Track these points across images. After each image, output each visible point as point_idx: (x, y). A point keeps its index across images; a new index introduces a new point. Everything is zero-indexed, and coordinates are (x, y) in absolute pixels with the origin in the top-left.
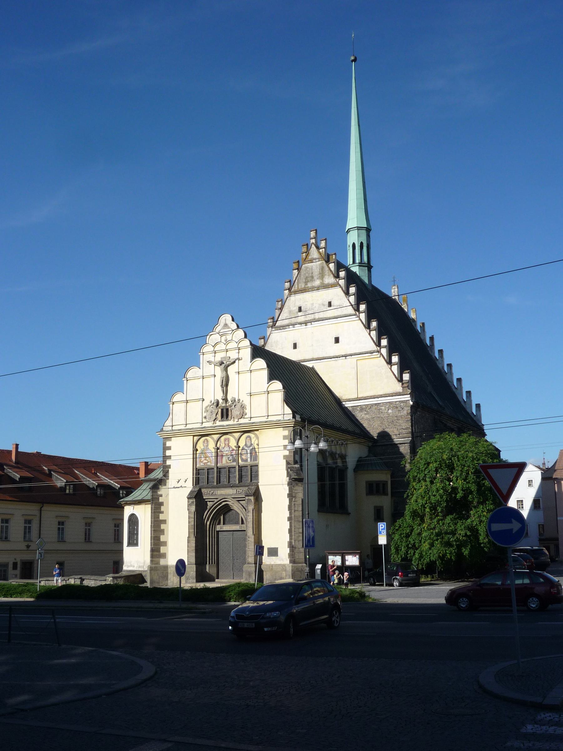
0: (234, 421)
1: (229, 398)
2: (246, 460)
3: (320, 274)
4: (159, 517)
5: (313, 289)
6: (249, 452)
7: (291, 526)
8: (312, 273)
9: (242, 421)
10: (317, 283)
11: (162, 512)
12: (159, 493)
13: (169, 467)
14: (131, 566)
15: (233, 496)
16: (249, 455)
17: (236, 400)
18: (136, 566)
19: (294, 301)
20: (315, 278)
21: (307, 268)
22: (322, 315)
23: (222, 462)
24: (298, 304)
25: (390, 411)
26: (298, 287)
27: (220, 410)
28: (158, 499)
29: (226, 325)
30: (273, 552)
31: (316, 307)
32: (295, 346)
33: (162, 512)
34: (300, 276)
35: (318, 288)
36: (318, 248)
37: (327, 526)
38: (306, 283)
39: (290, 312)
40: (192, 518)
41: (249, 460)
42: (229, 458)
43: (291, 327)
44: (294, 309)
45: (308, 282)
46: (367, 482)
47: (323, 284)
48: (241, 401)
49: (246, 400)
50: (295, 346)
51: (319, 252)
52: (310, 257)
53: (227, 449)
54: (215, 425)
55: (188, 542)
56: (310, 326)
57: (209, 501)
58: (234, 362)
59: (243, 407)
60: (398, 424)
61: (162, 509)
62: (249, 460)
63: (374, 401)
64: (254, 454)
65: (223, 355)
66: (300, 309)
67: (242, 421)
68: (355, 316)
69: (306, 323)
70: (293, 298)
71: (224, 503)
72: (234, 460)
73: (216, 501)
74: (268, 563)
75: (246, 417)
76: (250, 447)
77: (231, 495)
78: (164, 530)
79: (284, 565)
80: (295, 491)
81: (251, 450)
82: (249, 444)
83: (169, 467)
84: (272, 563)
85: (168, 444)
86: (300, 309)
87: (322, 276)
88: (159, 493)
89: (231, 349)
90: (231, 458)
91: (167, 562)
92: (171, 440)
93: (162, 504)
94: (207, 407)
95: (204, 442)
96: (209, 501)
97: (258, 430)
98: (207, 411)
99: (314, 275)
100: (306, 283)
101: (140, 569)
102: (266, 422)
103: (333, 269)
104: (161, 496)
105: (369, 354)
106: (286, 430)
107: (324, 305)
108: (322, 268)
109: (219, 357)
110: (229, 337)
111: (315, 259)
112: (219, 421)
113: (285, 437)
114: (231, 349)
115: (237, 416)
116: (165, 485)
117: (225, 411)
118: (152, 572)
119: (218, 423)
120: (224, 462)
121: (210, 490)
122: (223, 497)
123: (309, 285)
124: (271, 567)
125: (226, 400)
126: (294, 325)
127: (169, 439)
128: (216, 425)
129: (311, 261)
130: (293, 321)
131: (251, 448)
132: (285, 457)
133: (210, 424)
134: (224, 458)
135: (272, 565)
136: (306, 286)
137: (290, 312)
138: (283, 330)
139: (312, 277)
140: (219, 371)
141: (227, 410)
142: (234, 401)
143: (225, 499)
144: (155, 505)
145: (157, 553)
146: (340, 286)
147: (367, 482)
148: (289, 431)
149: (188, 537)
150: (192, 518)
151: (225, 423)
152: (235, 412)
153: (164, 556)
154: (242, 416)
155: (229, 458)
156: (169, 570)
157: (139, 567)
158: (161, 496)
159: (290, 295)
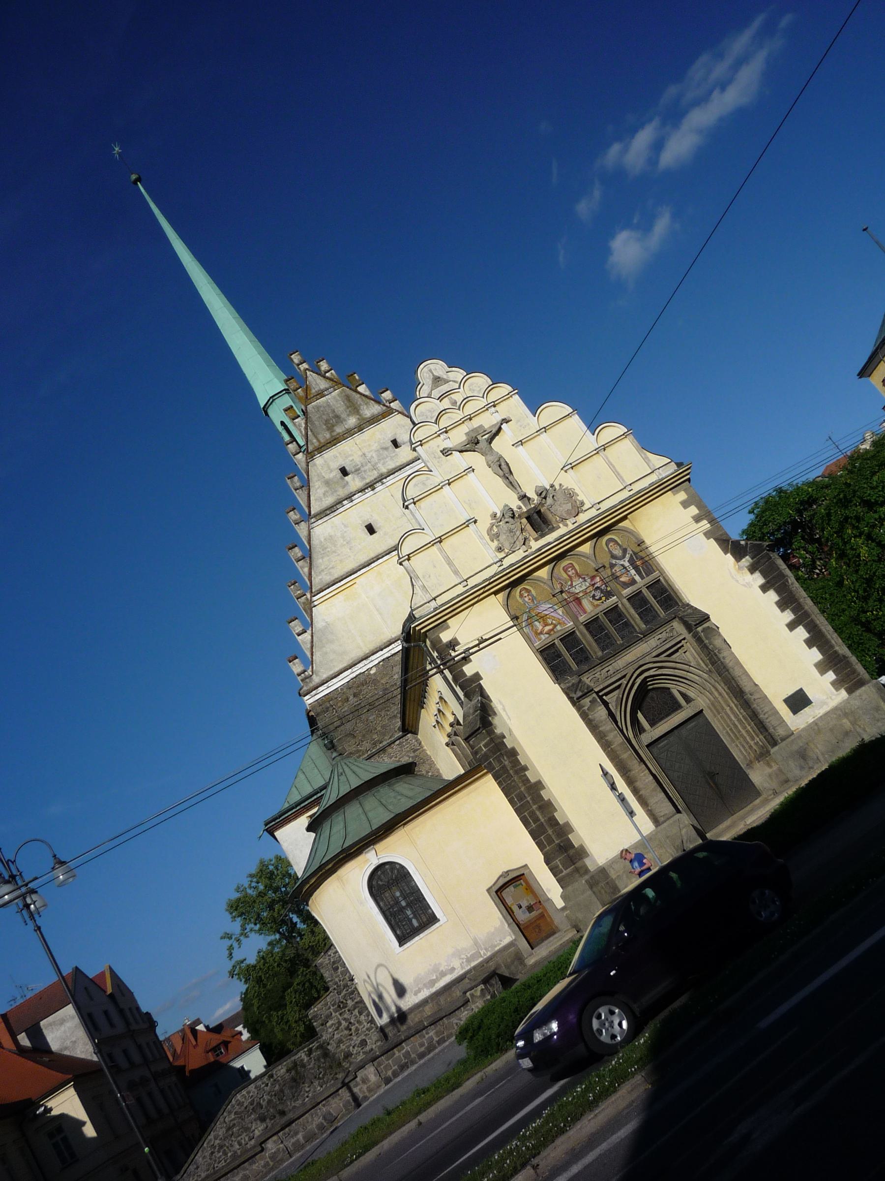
0: (567, 525)
1: (532, 494)
2: (633, 582)
3: (348, 408)
5: (350, 433)
6: (627, 564)
7: (812, 628)
8: (334, 411)
9: (583, 518)
10: (352, 421)
13: (477, 677)
14: (443, 974)
15: (654, 654)
16: (633, 572)
17: (548, 487)
18: (456, 963)
19: (325, 465)
20: (343, 416)
21: (318, 407)
22: (392, 465)
23: (585, 612)
24: (336, 465)
26: (318, 441)
27: (524, 521)
29: (437, 381)
30: (798, 701)
31: (372, 457)
32: (371, 529)
34: (313, 424)
36: (318, 372)
38: (330, 429)
39: (327, 483)
40: (611, 731)
41: (637, 578)
42: (594, 597)
43: (345, 502)
44: (332, 475)
45: (333, 426)
47: (364, 419)
48: (557, 487)
49: (569, 480)
50: (371, 529)
51: (328, 378)
52: (313, 391)
53: (577, 582)
54: (530, 551)
56: (372, 493)
57: (606, 694)
58: (500, 429)
59: (570, 495)
62: (637, 578)
64: (643, 561)
65: (464, 429)
66: (344, 472)
67: (583, 518)
69: (371, 486)
70: (319, 461)
71: (639, 681)
72: (608, 594)
73: (628, 677)
74: (802, 727)
75: (584, 508)
76: (624, 557)
77: (649, 653)
79: (836, 709)
81: (632, 562)
82: (618, 552)
83: (477, 677)
84: (811, 720)
85: (445, 637)
86: (344, 472)
87: (354, 409)
89: (477, 413)
90: (598, 594)
91: (594, 861)
92: (448, 627)
94: (491, 528)
95: (521, 596)
96: (606, 694)
97: (625, 518)
98: (494, 537)
99: (339, 413)
100: (330, 429)
101: (473, 964)
102: (631, 497)
103: (367, 393)
106: (678, 492)
107: (386, 449)
108: (348, 398)
109: (459, 436)
110: (458, 397)
111: (327, 389)
112: (536, 540)
113: (685, 504)
114: (477, 413)
115: (568, 512)
116: (495, 714)
117: (536, 516)
118: (594, 889)
119: (535, 545)
120: (590, 608)
121: (598, 669)
122: (636, 666)
123: (339, 430)
124: (815, 728)
125: (523, 497)
126: (350, 497)
127: (442, 625)
128: (533, 549)
129: (321, 394)
130: (342, 493)
131: (628, 556)
132: (708, 535)
133: (519, 554)
134: (586, 603)
135: (815, 723)
136: (335, 434)
137: (327, 483)
138: (332, 515)
139: (337, 417)
140: (475, 459)
141: (539, 513)
142: (543, 494)
143: (641, 668)
144: (508, 757)
146: (397, 411)
148: (685, 490)
150: (611, 731)
151: (550, 537)
152: (557, 508)
153: (582, 853)
154: (578, 509)
155: (594, 597)
156: (613, 874)
157: (469, 960)
159: (310, 456)
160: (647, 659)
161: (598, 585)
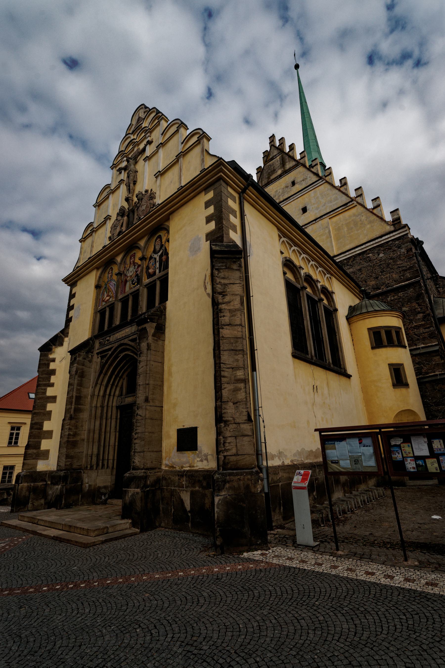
4: (45, 393)
6: (158, 259)
10: (279, 172)
11: (52, 385)
12: (51, 356)
15: (131, 338)
17: (144, 193)
23: (124, 292)
25: (381, 255)
28: (48, 365)
33: (52, 385)
35: (280, 176)
37: (315, 388)
38: (269, 178)
46: (369, 329)
55: (62, 429)
60: (396, 267)
61: (53, 379)
63: (358, 251)
68: (321, 181)
78: (50, 412)
80: (223, 281)
81: (161, 257)
88: (51, 356)
93: (53, 372)
104: (54, 360)
105: (343, 207)
122: (119, 343)
145: (35, 451)
147: (369, 329)
149: (64, 420)
158: (54, 360)
160: (126, 341)
161: (138, 273)
